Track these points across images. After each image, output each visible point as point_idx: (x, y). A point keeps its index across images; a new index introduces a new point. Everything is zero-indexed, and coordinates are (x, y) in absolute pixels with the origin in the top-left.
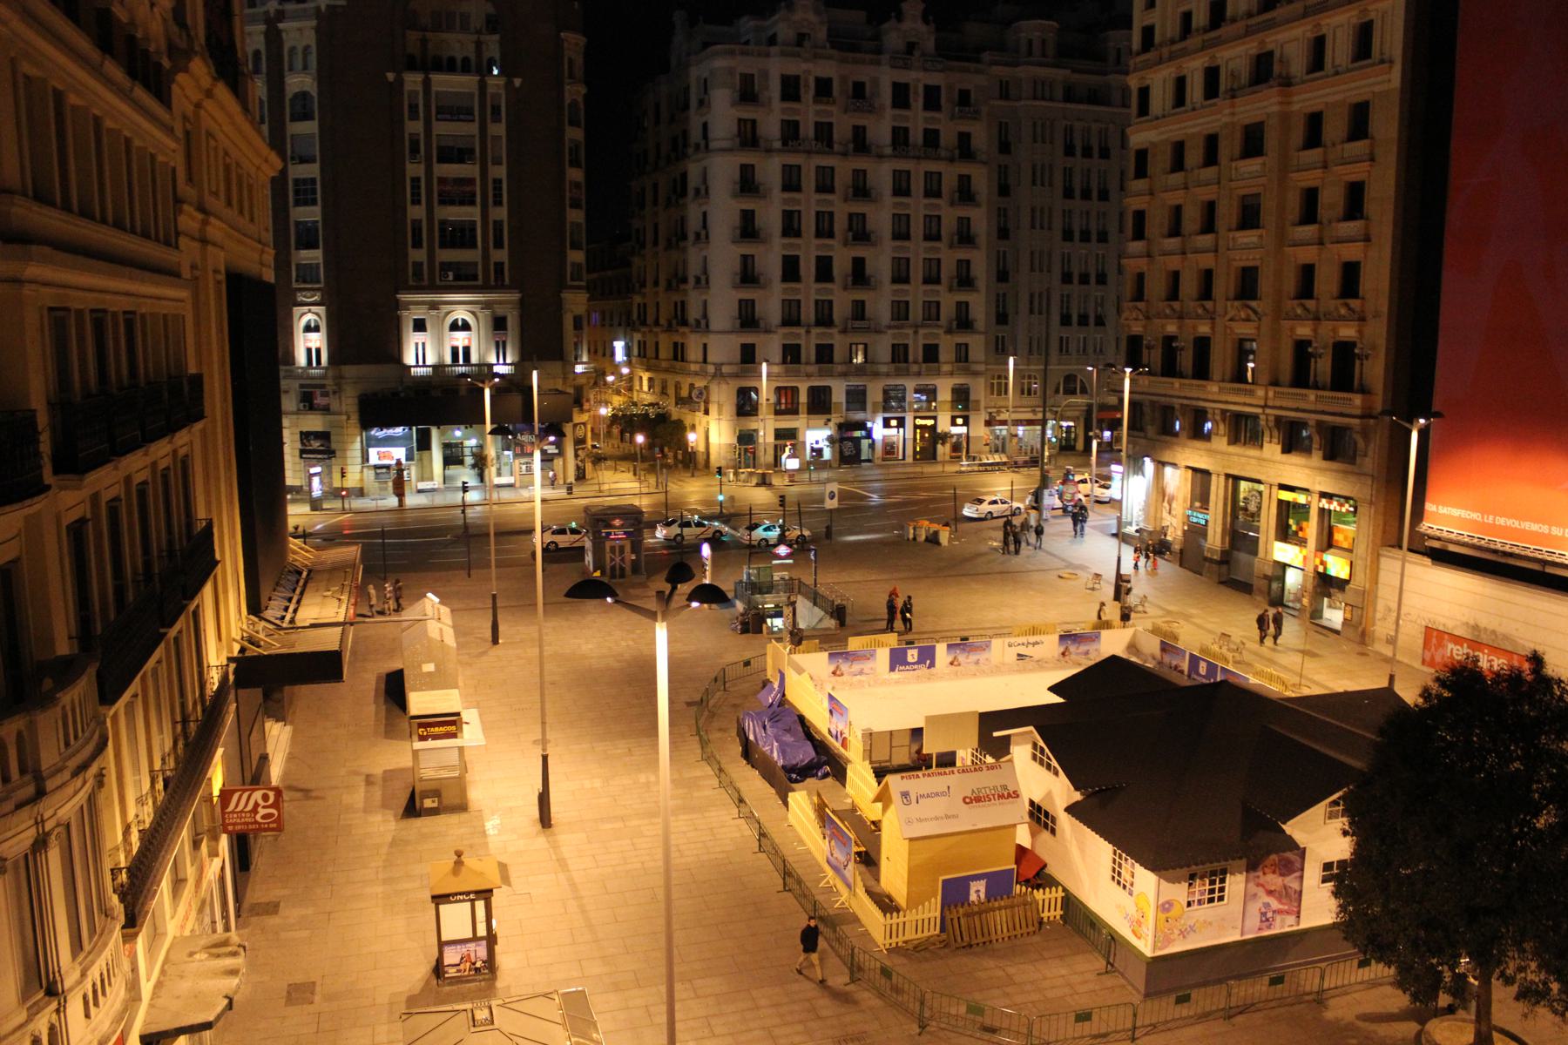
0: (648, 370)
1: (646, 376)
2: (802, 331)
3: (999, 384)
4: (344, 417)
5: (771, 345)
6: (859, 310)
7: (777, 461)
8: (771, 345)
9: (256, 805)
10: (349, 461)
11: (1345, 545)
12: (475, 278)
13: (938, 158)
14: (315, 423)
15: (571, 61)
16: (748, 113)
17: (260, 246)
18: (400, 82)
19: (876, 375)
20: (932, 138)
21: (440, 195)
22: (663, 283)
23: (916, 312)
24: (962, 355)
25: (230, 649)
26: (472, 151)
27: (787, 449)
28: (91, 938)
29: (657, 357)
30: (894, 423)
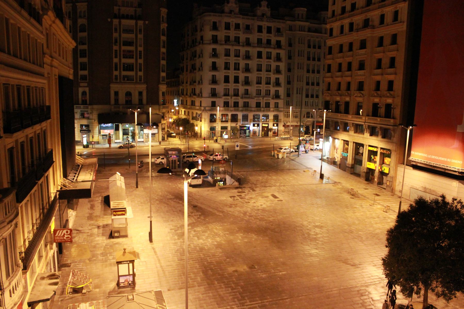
0: (184, 108)
1: (183, 110)
2: (229, 97)
3: (287, 114)
4: (94, 120)
5: (220, 101)
6: (247, 92)
7: (221, 136)
8: (220, 101)
9: (64, 234)
10: (95, 133)
11: (388, 163)
12: (134, 80)
13: (271, 48)
14: (85, 122)
15: (163, 17)
16: (215, 33)
17: (69, 69)
18: (112, 22)
19: (251, 111)
20: (269, 42)
21: (123, 55)
22: (189, 83)
23: (263, 93)
24: (277, 105)
25: (57, 188)
26: (133, 42)
27: (224, 132)
28: (12, 272)
29: (187, 105)
30: (256, 125)
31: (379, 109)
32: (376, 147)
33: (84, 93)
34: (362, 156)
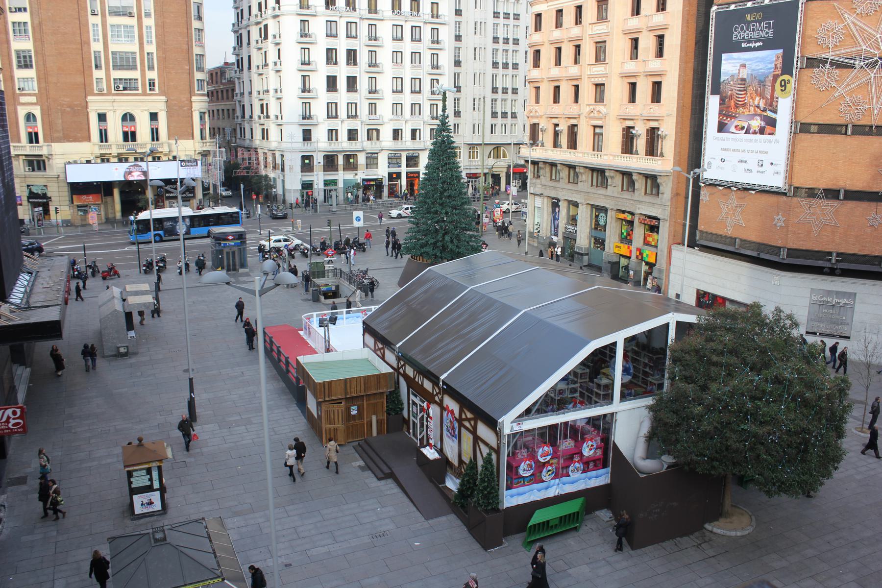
9: (9, 418)
11: (653, 244)
12: (138, 90)
31: (635, 138)
32: (632, 214)
33: (30, 117)
34: (605, 231)
